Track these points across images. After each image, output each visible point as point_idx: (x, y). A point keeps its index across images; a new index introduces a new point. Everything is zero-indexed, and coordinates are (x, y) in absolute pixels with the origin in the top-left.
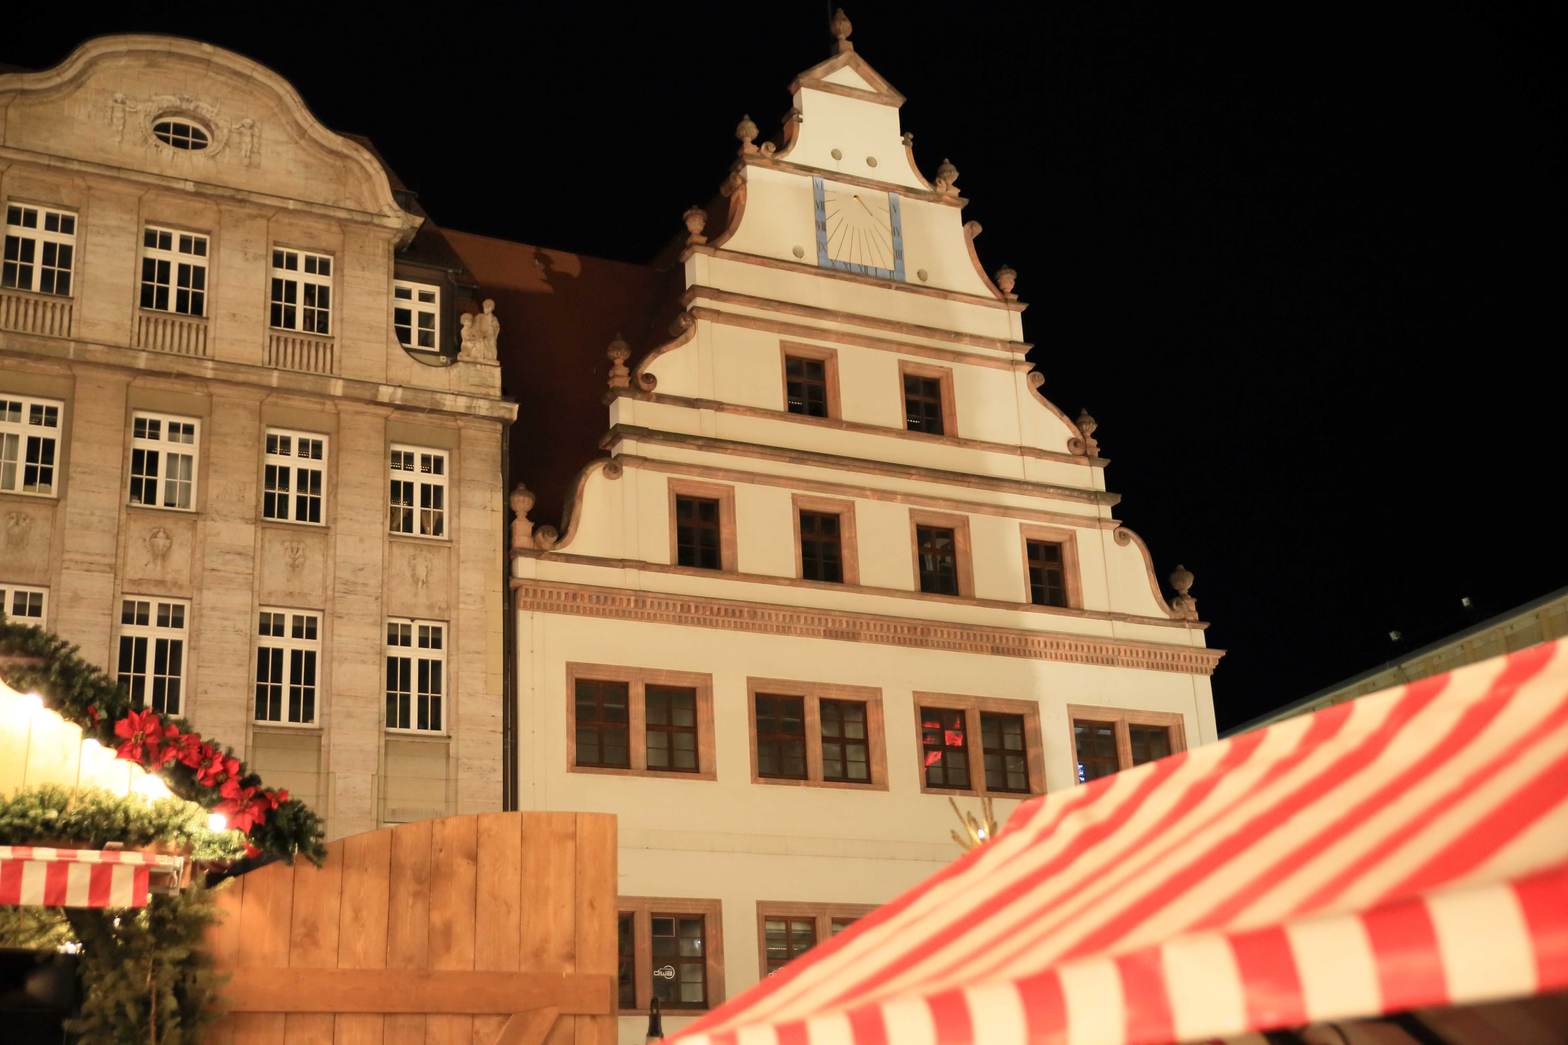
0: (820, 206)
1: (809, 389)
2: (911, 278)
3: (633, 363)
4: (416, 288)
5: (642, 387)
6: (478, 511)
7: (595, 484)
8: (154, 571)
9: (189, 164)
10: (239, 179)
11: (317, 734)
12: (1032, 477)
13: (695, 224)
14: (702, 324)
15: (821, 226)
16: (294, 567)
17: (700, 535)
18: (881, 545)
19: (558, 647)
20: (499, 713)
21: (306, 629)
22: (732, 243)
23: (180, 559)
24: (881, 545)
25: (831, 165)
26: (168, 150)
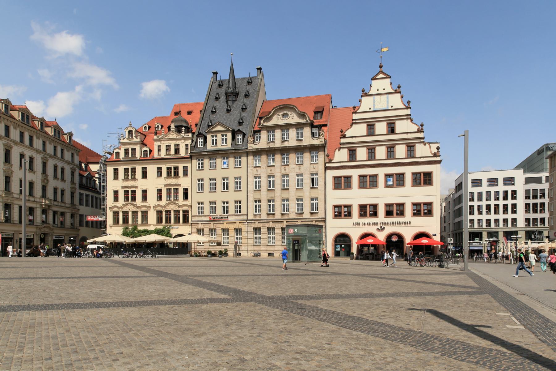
8: (285, 172)
11: (302, 188)
16: (300, 169)
18: (381, 152)
23: (287, 171)
24: (381, 152)
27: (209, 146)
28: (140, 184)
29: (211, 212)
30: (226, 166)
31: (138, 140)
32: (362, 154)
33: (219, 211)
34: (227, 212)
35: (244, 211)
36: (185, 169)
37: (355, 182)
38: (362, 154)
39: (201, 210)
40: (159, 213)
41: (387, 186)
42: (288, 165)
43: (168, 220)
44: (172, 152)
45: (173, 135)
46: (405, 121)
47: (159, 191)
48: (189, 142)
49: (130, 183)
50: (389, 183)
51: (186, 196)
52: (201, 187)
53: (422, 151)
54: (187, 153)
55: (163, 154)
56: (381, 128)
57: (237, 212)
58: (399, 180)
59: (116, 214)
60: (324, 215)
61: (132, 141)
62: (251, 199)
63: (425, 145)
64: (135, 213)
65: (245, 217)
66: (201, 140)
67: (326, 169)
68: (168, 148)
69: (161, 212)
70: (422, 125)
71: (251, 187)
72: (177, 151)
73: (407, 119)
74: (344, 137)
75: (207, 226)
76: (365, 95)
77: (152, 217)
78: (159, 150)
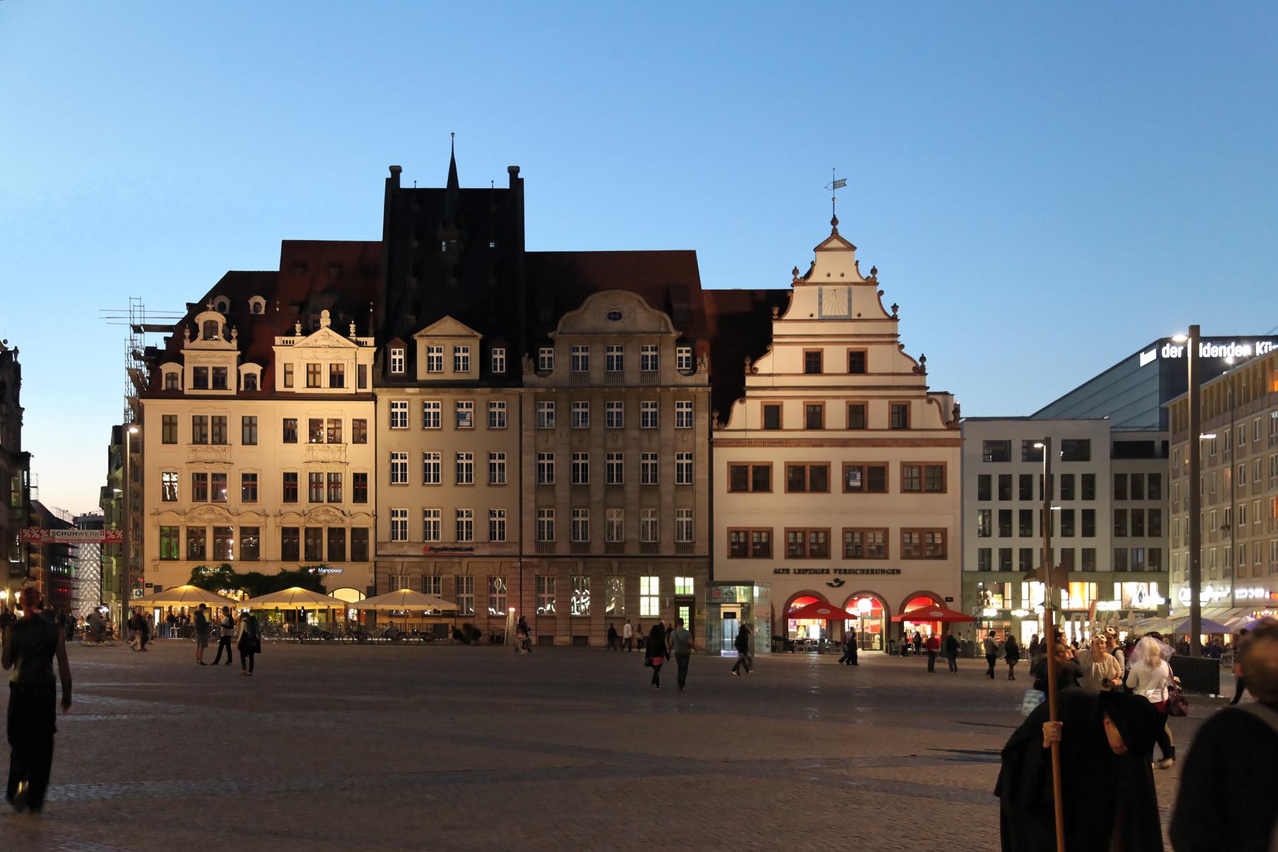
0: (820, 296)
1: (813, 363)
2: (855, 316)
3: (751, 365)
4: (684, 349)
5: (754, 372)
6: (702, 421)
7: (737, 407)
9: (617, 325)
10: (631, 328)
12: (896, 384)
13: (776, 311)
14: (776, 348)
15: (820, 304)
17: (772, 417)
18: (836, 414)
19: (724, 457)
20: (707, 477)
21: (654, 457)
22: (787, 317)
24: (836, 414)
25: (826, 280)
26: (611, 322)
27: (422, 374)
28: (238, 459)
29: (426, 536)
30: (465, 424)
31: (234, 344)
32: (793, 414)
33: (446, 536)
34: (469, 536)
35: (511, 533)
36: (359, 425)
37: (779, 478)
38: (793, 414)
39: (398, 530)
40: (289, 534)
41: (848, 489)
42: (622, 430)
43: (312, 554)
44: (325, 379)
45: (325, 334)
46: (890, 347)
47: (290, 480)
48: (367, 356)
49: (208, 452)
50: (854, 483)
51: (360, 495)
52: (397, 474)
53: (924, 416)
54: (361, 382)
55: (299, 386)
56: (835, 359)
57: (492, 536)
58: (874, 479)
59: (169, 534)
60: (707, 549)
61: (215, 345)
62: (529, 505)
63: (930, 401)
64: (222, 533)
65: (515, 550)
66: (398, 355)
67: (712, 444)
68: (312, 372)
69: (296, 531)
70: (923, 359)
71: (529, 478)
72: (337, 379)
73: (892, 343)
74: (754, 372)
75: (418, 570)
76: (804, 280)
77: (271, 545)
78: (288, 373)
